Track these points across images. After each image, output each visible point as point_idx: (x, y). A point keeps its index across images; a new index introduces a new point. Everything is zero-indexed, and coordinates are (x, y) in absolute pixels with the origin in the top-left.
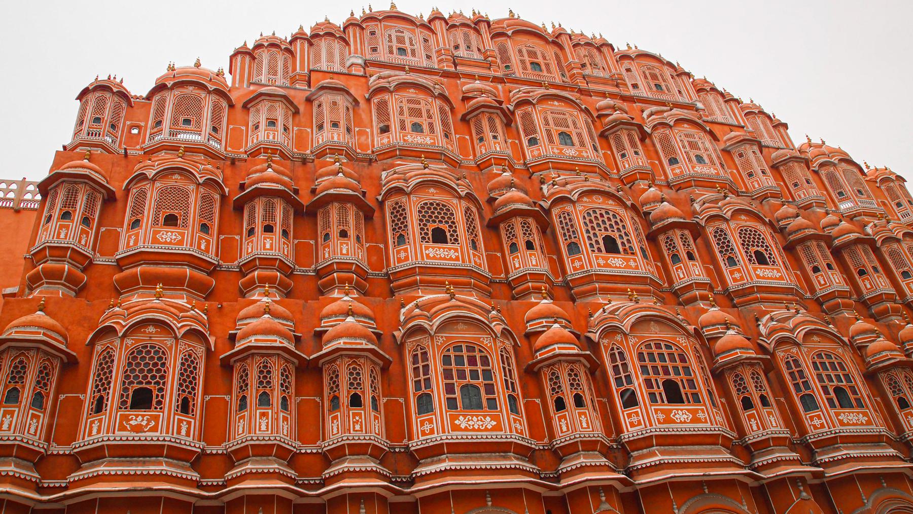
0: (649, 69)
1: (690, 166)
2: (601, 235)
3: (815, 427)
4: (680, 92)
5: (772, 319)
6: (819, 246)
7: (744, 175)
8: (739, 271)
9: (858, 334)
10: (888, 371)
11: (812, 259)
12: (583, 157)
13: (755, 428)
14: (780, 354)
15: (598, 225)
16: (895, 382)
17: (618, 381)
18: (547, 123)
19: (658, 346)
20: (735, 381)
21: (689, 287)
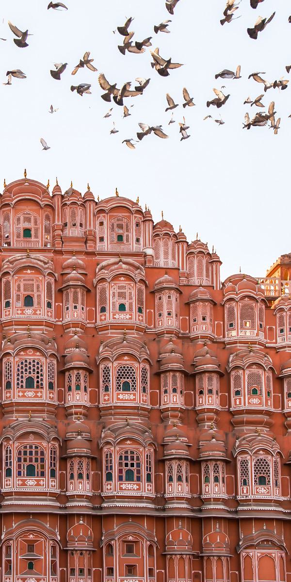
0: (118, 220)
1: (111, 314)
2: (26, 375)
3: (107, 489)
4: (138, 240)
5: (109, 429)
6: (174, 376)
7: (157, 314)
8: (108, 395)
9: (166, 437)
10: (171, 460)
11: (166, 385)
12: (37, 314)
13: (71, 489)
14: (105, 450)
15: (26, 370)
16: (172, 467)
17: (7, 463)
18: (19, 290)
19: (31, 447)
20: (71, 464)
21: (71, 407)
